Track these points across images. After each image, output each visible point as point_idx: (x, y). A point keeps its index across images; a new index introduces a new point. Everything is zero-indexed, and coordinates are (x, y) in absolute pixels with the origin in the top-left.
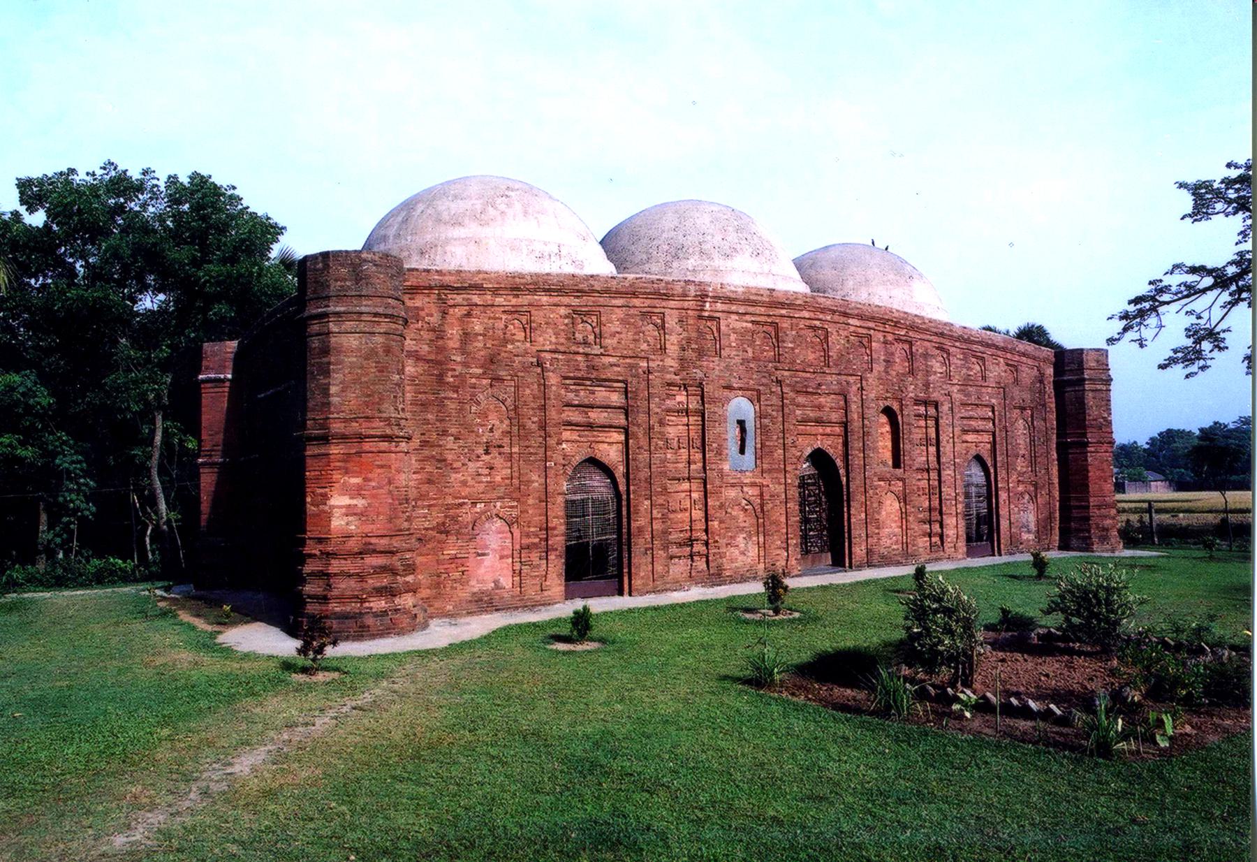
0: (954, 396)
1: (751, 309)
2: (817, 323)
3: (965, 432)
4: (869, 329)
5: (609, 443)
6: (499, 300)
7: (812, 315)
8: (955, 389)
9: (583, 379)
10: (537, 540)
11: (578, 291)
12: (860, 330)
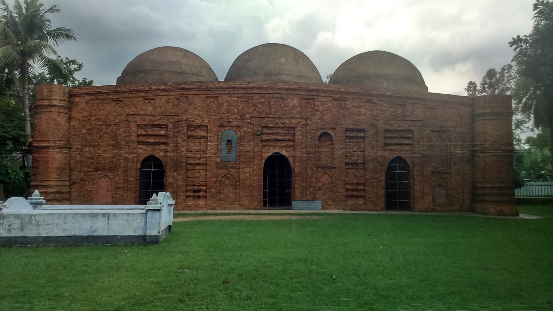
0: (379, 125)
1: (235, 92)
2: (278, 96)
3: (386, 144)
6: (111, 97)
7: (274, 92)
8: (380, 122)
9: (148, 125)
10: (122, 186)
11: (145, 91)
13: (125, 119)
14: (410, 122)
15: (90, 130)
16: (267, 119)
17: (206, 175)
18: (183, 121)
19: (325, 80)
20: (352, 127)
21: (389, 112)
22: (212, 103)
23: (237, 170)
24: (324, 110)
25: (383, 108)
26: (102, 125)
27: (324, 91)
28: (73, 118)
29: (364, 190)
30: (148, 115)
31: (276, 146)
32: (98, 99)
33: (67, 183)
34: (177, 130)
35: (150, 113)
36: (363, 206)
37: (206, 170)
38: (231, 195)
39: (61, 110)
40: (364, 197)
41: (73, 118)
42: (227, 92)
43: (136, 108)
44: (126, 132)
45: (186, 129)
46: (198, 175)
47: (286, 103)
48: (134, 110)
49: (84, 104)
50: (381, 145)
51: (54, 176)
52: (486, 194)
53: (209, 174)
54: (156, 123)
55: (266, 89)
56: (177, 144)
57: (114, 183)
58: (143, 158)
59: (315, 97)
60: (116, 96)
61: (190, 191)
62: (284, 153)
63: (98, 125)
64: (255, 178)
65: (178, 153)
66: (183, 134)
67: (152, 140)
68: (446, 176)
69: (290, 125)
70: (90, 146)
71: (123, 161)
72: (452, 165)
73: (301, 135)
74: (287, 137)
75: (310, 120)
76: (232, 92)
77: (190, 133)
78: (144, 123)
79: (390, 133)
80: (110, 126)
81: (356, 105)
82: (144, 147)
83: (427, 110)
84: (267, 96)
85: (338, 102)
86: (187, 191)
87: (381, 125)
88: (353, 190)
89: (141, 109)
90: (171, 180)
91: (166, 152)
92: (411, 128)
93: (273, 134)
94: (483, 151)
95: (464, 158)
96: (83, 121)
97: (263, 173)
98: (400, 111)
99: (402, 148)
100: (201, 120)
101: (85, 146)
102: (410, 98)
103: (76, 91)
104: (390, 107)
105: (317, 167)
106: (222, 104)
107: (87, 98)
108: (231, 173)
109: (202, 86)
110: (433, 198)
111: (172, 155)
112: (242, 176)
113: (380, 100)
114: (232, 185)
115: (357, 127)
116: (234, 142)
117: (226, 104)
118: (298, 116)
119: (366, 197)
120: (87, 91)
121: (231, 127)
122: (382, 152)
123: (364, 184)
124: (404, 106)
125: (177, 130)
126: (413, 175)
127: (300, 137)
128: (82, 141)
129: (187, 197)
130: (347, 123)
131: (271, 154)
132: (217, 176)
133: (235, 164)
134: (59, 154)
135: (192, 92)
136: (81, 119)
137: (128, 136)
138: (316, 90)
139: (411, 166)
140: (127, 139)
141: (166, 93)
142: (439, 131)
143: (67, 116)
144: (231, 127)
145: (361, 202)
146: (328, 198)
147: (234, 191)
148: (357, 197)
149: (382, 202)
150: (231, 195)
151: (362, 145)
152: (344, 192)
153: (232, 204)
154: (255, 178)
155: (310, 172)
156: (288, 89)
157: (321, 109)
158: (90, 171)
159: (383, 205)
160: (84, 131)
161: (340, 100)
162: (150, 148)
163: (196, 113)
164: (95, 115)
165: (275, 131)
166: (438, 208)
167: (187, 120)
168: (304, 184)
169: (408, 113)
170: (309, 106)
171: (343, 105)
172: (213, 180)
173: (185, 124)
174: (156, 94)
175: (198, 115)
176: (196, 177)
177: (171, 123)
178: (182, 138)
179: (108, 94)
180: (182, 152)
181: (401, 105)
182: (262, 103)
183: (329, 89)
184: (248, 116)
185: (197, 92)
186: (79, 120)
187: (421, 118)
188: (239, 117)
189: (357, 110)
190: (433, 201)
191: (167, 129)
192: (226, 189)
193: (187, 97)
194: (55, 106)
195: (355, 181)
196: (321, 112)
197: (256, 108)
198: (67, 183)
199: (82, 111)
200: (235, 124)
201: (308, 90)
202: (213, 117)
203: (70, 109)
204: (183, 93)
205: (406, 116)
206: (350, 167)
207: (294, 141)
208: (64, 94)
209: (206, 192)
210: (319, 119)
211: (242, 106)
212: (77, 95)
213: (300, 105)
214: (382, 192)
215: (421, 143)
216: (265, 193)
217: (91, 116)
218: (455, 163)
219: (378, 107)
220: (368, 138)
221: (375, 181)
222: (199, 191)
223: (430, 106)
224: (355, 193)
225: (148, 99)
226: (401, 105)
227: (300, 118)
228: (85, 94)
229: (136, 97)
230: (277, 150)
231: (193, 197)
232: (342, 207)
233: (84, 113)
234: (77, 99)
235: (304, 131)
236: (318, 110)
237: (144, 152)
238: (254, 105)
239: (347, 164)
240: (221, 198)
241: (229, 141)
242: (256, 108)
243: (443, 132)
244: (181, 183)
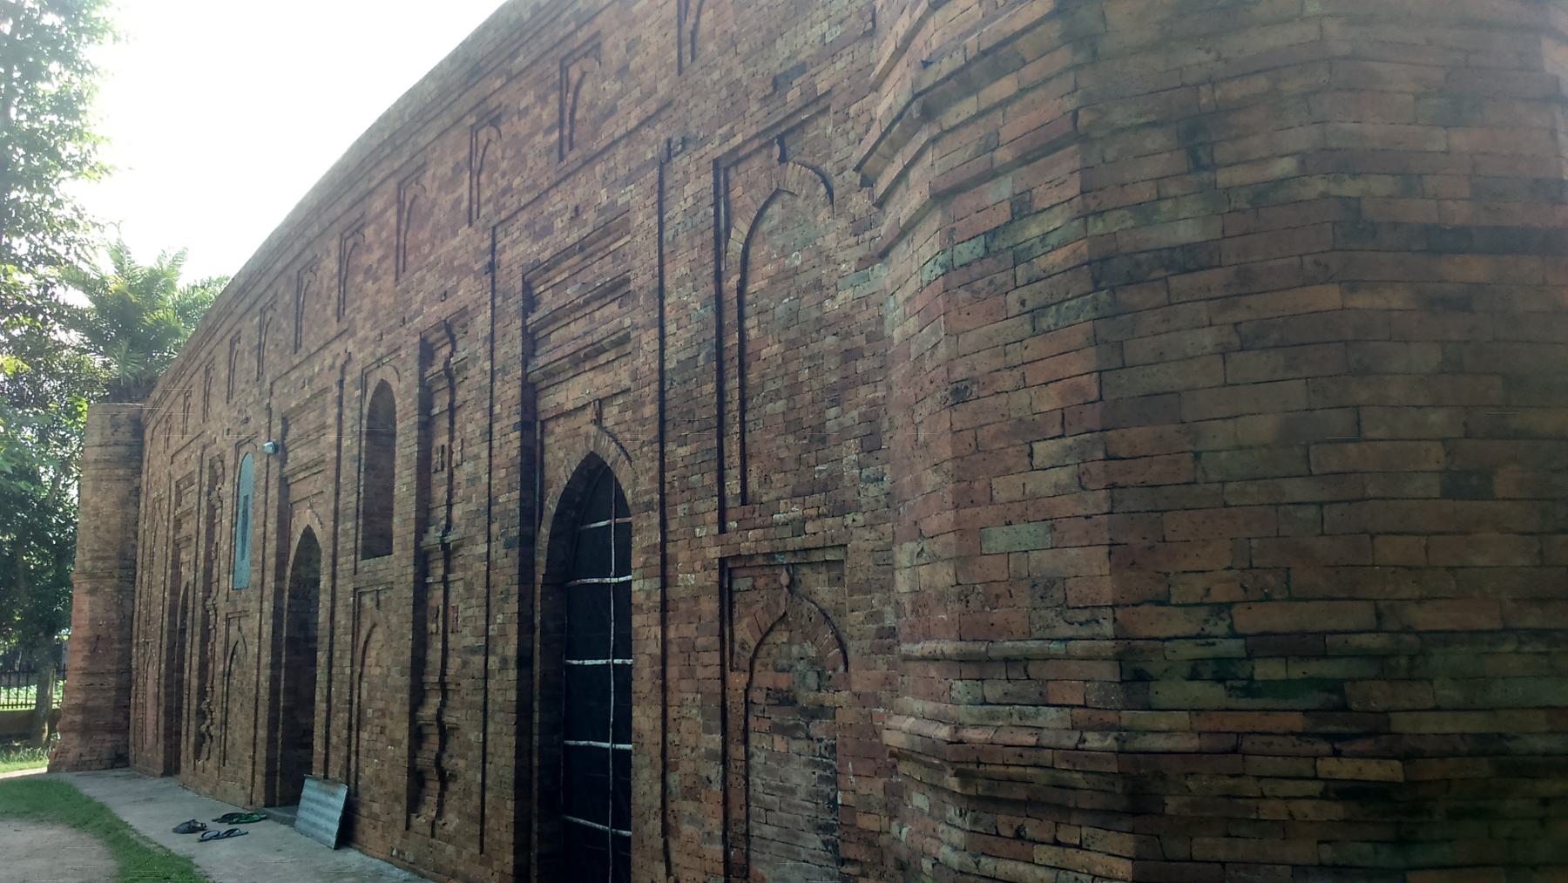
2: (308, 255)
14: (621, 152)
20: (436, 312)
21: (539, 138)
24: (380, 261)
33: (112, 681)
62: (317, 530)
68: (820, 588)
81: (445, 170)
118: (333, 328)
130: (423, 303)
187: (663, 89)
208: (116, 427)
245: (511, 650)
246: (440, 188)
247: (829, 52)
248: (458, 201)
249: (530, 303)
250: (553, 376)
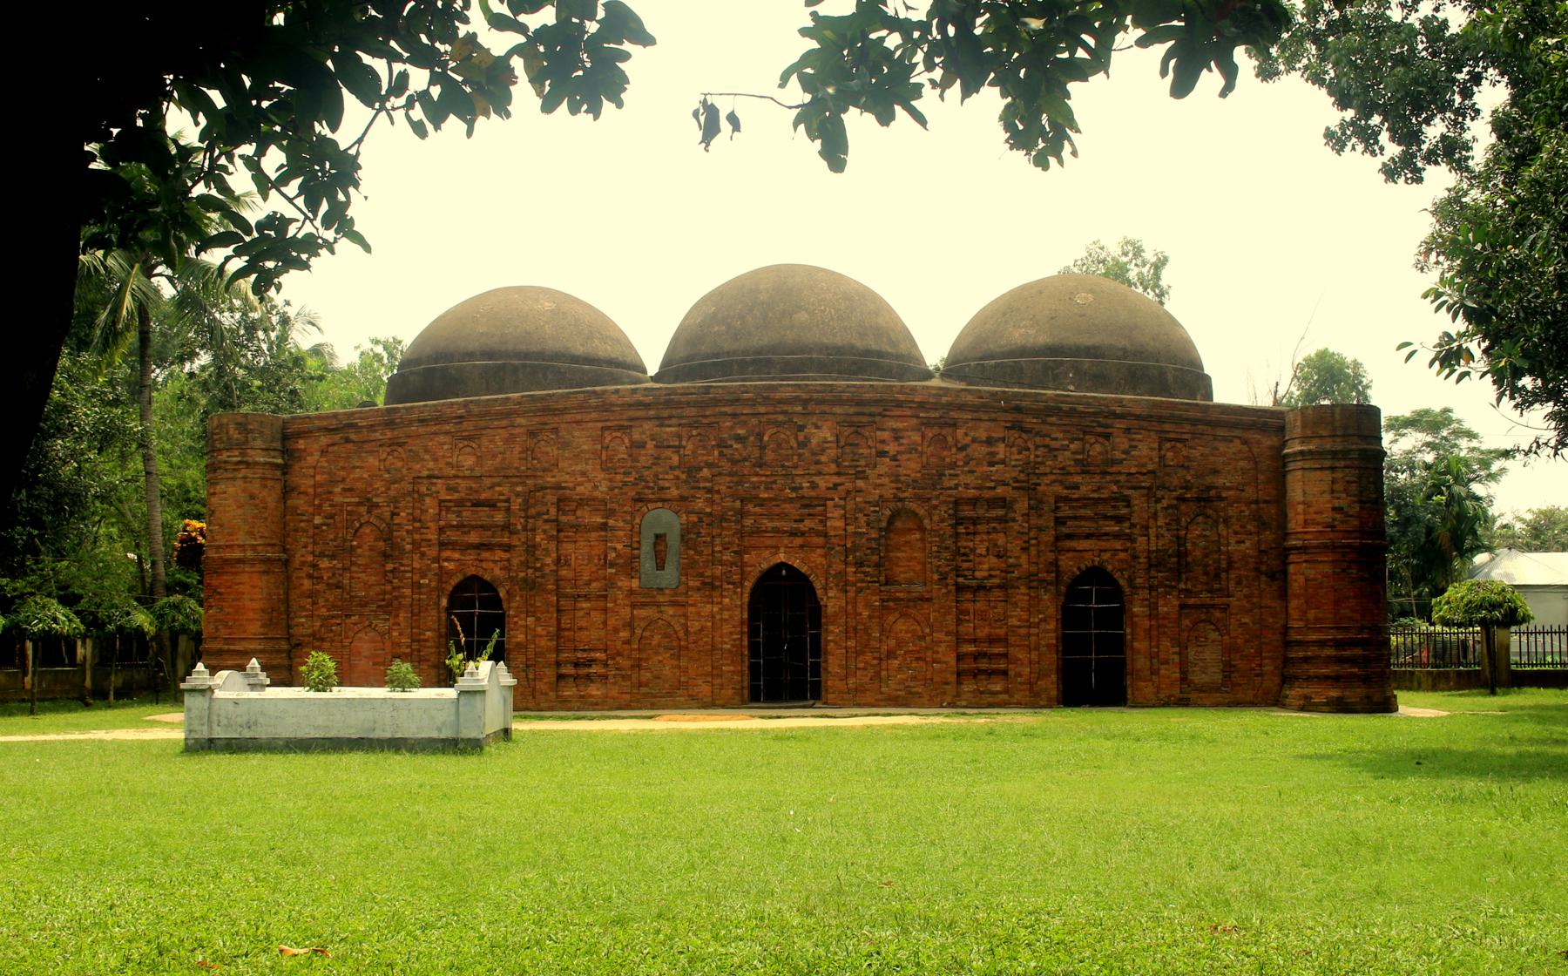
1: (675, 412)
2: (781, 418)
4: (871, 415)
5: (495, 562)
6: (378, 435)
7: (770, 409)
8: (1046, 480)
12: (856, 419)
13: (410, 487)
15: (332, 517)
16: (755, 479)
17: (605, 623)
18: (543, 488)
19: (934, 349)
20: (972, 492)
22: (618, 441)
23: (680, 611)
25: (1054, 444)
26: (359, 504)
27: (899, 404)
28: (293, 489)
29: (1005, 655)
30: (464, 477)
31: (777, 548)
32: (348, 441)
34: (533, 511)
35: (467, 473)
36: (1005, 697)
37: (606, 610)
38: (667, 671)
39: (268, 474)
40: (1005, 673)
41: (293, 489)
42: (652, 413)
43: (436, 460)
44: (414, 520)
45: (553, 511)
46: (583, 623)
47: (801, 438)
48: (431, 465)
49: (317, 455)
50: (1048, 537)
51: (255, 628)
52: (1306, 660)
53: (612, 622)
54: (483, 497)
55: (753, 403)
56: (531, 548)
57: (388, 644)
58: (455, 581)
59: (877, 419)
60: (389, 435)
61: (567, 662)
62: (796, 564)
63: (349, 504)
64: (727, 628)
65: (536, 569)
66: (546, 521)
67: (473, 538)
68: (1218, 614)
69: (813, 494)
70: (333, 557)
71: (408, 592)
72: (1232, 586)
73: (844, 517)
74: (808, 523)
75: (866, 478)
76: (665, 413)
77: (564, 519)
78: (456, 496)
79: (1071, 508)
80: (377, 506)
81: (983, 435)
82: (457, 556)
83: (1168, 445)
84: (754, 421)
85: (936, 430)
86: (558, 664)
87: (1049, 488)
88: (976, 657)
89: (448, 464)
90: (521, 638)
91: (507, 569)
92: (1126, 492)
93: (771, 517)
94: (1303, 549)
95: (1264, 568)
96: (316, 495)
97: (746, 615)
98: (1098, 448)
99: (1103, 545)
100: (589, 486)
101: (322, 555)
102: (1122, 417)
103: (294, 428)
104: (1072, 441)
105: (882, 600)
106: (642, 445)
107: (324, 440)
108: (665, 617)
109: (593, 402)
110: (1182, 672)
111: (522, 575)
112: (695, 626)
113: (1044, 422)
114: (668, 649)
115: (987, 494)
116: (674, 541)
117: (650, 444)
119: (1012, 673)
120: (325, 423)
121: (664, 500)
122: (1051, 556)
123: (1003, 640)
124: (1107, 436)
125: (533, 511)
126: (1134, 615)
127: (841, 524)
128: (315, 543)
129: (560, 677)
131: (765, 566)
132: (630, 625)
133: (676, 595)
134: (265, 577)
135: (568, 417)
136: (311, 490)
137: (416, 530)
138: (877, 402)
139: (1127, 590)
140: (417, 537)
141: (504, 423)
142: (1198, 500)
143: (278, 486)
144: (664, 500)
145: (998, 688)
146: (914, 678)
147: (675, 663)
148: (990, 673)
149: (1050, 684)
150: (667, 671)
151: (1001, 540)
152: (953, 662)
153: (670, 694)
154: (727, 628)
155: (866, 613)
156: (805, 402)
157: (892, 448)
158: (333, 617)
159: (1054, 693)
160: (318, 520)
161: (941, 426)
162: (470, 556)
163: (579, 468)
164: (344, 480)
165: (777, 510)
166: (1193, 696)
167: (558, 487)
168: (851, 643)
169: (1118, 455)
170: (863, 442)
171: (950, 439)
172: (624, 634)
173: (551, 498)
174: (482, 424)
175: (583, 474)
176: (581, 629)
177: (518, 495)
178: (545, 531)
179: (371, 428)
180: (543, 565)
181: (1100, 435)
182: (739, 439)
183: (910, 398)
184: (706, 472)
185: (579, 417)
186: (306, 493)
187: (1150, 467)
188: (683, 476)
189: (985, 449)
190: (1183, 679)
191: (508, 509)
192: (656, 659)
193: (555, 430)
194: (257, 463)
195: (982, 633)
196: (894, 459)
197: (726, 451)
198: (284, 646)
199: (312, 471)
200: (674, 492)
201: (860, 403)
202: (619, 477)
203: (285, 469)
204: (546, 419)
205: (1114, 462)
206: (969, 596)
207: (826, 535)
209: (606, 665)
210: (886, 475)
211: (690, 446)
212: (300, 434)
213: (838, 441)
214: (1051, 660)
215: (1152, 531)
216: (754, 669)
217: (335, 482)
218: (1239, 583)
219: (1038, 439)
220: (1014, 520)
221: (1033, 631)
222: (590, 663)
223: (1172, 436)
224: (983, 664)
225: (464, 439)
226: (1100, 435)
227: (838, 474)
228: (319, 429)
229: (435, 433)
230: (782, 557)
231: (576, 678)
232: (949, 699)
233: (318, 478)
234: (301, 444)
235: (850, 505)
236: (882, 454)
237: (457, 564)
238: (722, 444)
239: (960, 589)
240: (643, 679)
241: (659, 538)
242: (726, 451)
243: (1208, 500)
244: (544, 643)
245: (1052, 625)
246: (974, 440)
247: (1229, 489)
248: (993, 454)
249: (1057, 508)
250: (1069, 537)
